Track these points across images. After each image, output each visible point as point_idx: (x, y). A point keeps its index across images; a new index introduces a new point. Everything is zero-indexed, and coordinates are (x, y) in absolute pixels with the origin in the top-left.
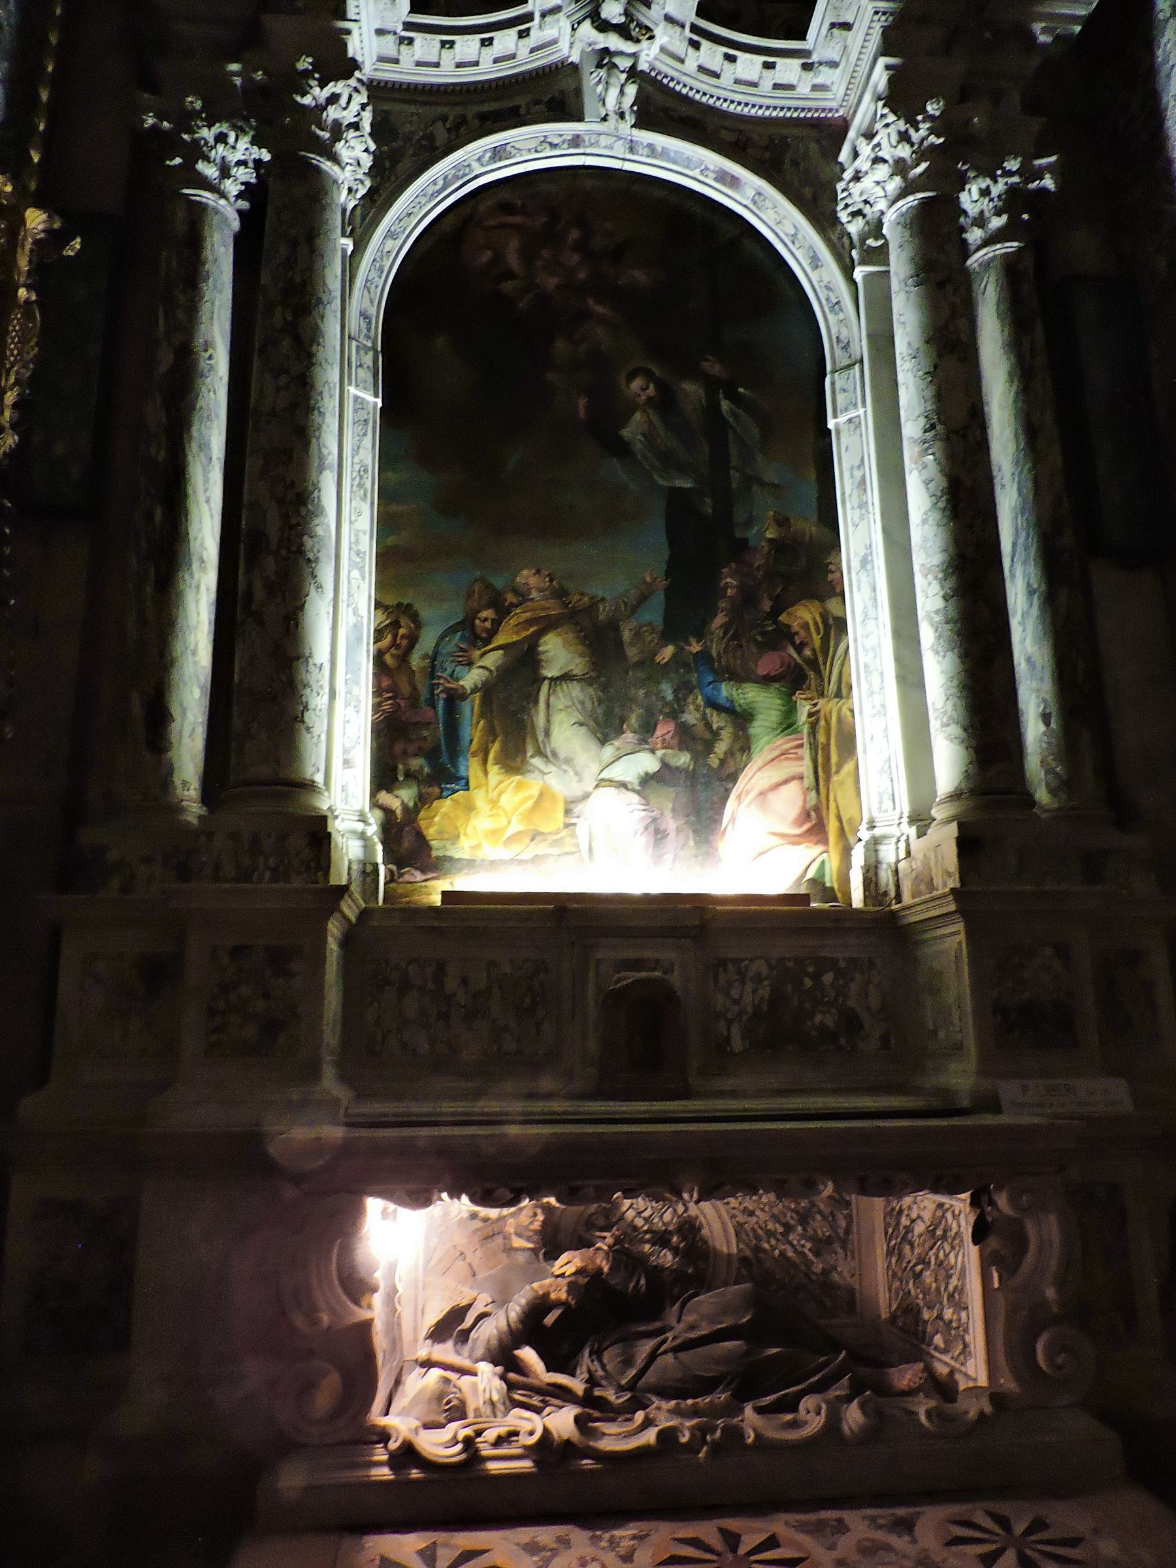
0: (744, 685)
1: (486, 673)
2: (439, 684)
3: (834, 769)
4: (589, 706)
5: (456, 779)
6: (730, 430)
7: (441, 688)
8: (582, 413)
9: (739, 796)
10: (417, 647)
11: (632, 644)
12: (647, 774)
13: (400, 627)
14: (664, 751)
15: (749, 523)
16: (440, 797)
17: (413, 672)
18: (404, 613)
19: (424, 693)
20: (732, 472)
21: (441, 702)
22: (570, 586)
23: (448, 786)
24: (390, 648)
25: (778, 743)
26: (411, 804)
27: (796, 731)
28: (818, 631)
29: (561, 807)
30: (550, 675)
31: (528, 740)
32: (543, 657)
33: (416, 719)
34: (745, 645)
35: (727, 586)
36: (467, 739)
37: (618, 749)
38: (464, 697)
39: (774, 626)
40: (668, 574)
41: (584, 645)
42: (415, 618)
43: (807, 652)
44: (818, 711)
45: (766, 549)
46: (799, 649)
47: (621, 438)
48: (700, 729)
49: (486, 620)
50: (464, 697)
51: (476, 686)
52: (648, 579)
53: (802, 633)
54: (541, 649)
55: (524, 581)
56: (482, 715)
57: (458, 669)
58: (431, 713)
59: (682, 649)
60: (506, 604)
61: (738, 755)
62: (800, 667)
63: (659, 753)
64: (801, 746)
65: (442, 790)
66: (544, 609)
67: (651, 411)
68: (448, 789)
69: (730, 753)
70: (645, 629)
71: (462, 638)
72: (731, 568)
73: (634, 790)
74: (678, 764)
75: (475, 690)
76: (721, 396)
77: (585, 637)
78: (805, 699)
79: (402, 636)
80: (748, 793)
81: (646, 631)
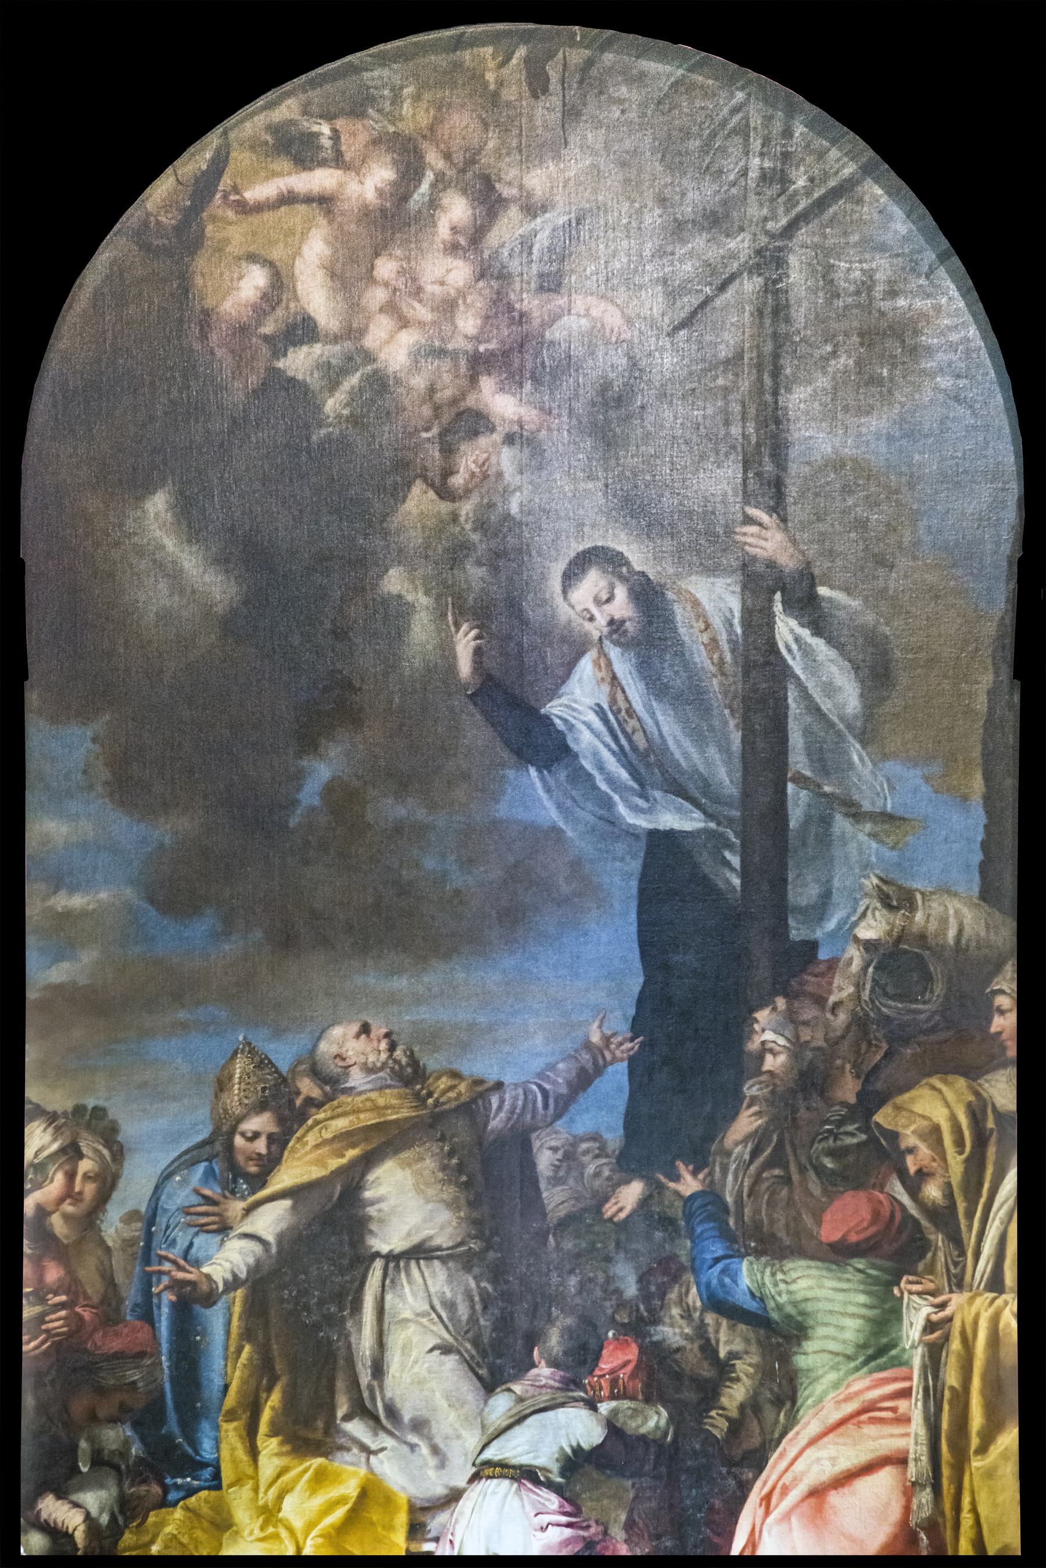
0: (789, 1265)
1: (257, 1248)
2: (161, 1273)
3: (975, 1442)
4: (463, 1311)
5: (194, 1466)
6: (791, 687)
7: (165, 1280)
8: (465, 666)
9: (767, 1499)
10: (116, 1196)
11: (556, 1181)
12: (578, 1450)
13: (81, 1156)
14: (613, 1404)
15: (821, 908)
16: (163, 1503)
17: (108, 1250)
18: (88, 1126)
19: (131, 1294)
20: (790, 787)
21: (165, 1310)
22: (431, 1062)
23: (179, 1481)
24: (61, 1200)
25: (857, 1386)
26: (105, 1519)
27: (898, 1362)
28: (959, 1143)
29: (402, 1519)
30: (385, 1249)
31: (340, 1384)
32: (371, 1211)
33: (115, 1345)
34: (796, 1177)
35: (765, 1049)
36: (218, 1382)
37: (520, 1400)
38: (210, 1299)
39: (864, 1137)
40: (637, 1026)
41: (457, 1184)
42: (109, 1135)
43: (933, 1191)
44: (950, 1319)
45: (856, 966)
46: (914, 1184)
47: (546, 721)
48: (692, 1356)
49: (256, 1135)
50: (210, 1299)
51: (235, 1276)
52: (595, 1038)
53: (924, 1151)
54: (368, 1194)
55: (334, 1049)
56: (247, 1335)
57: (200, 1240)
58: (144, 1333)
59: (661, 1187)
60: (298, 1102)
61: (769, 1413)
62: (916, 1222)
63: (604, 1408)
64: (906, 1393)
65: (166, 1490)
66: (376, 1108)
67: (614, 652)
68: (177, 1487)
69: (752, 1406)
70: (584, 1146)
71: (209, 1174)
72: (774, 1009)
73: (550, 1485)
74: (643, 1430)
75: (233, 1284)
76: (778, 607)
77: (460, 1168)
78: (919, 1294)
79: (86, 1177)
80: (785, 1491)
81: (586, 1152)
